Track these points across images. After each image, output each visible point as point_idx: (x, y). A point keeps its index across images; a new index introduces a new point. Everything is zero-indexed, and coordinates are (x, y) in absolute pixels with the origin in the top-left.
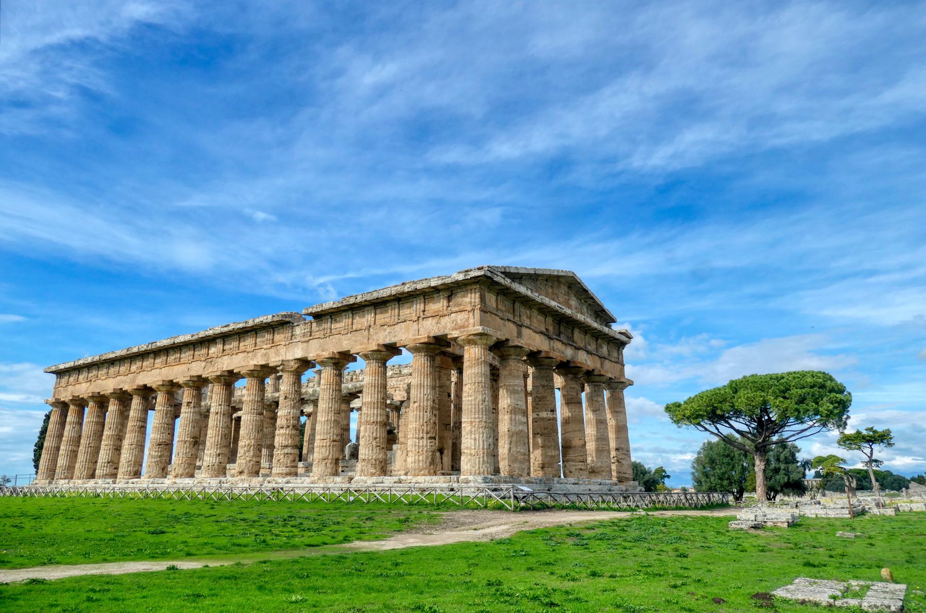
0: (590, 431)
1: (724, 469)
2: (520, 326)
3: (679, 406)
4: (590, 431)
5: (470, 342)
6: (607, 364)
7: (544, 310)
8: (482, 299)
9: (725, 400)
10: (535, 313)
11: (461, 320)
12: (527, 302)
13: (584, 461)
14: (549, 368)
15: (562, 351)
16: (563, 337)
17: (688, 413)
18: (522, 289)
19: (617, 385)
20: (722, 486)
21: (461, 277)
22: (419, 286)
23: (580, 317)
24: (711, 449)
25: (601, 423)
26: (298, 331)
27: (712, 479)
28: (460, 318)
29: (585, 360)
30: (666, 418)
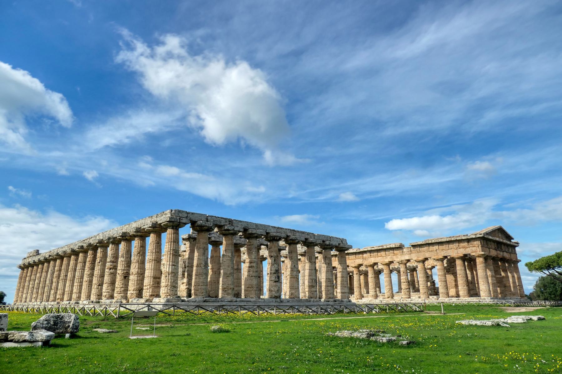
0: (511, 280)
1: (551, 290)
3: (532, 264)
5: (479, 256)
6: (512, 255)
9: (554, 262)
11: (475, 250)
13: (511, 291)
14: (498, 261)
15: (501, 254)
17: (537, 267)
18: (490, 237)
20: (551, 298)
21: (474, 237)
22: (458, 239)
24: (544, 280)
25: (513, 277)
26: (405, 250)
27: (545, 294)
28: (474, 249)
29: (506, 255)
30: (526, 268)
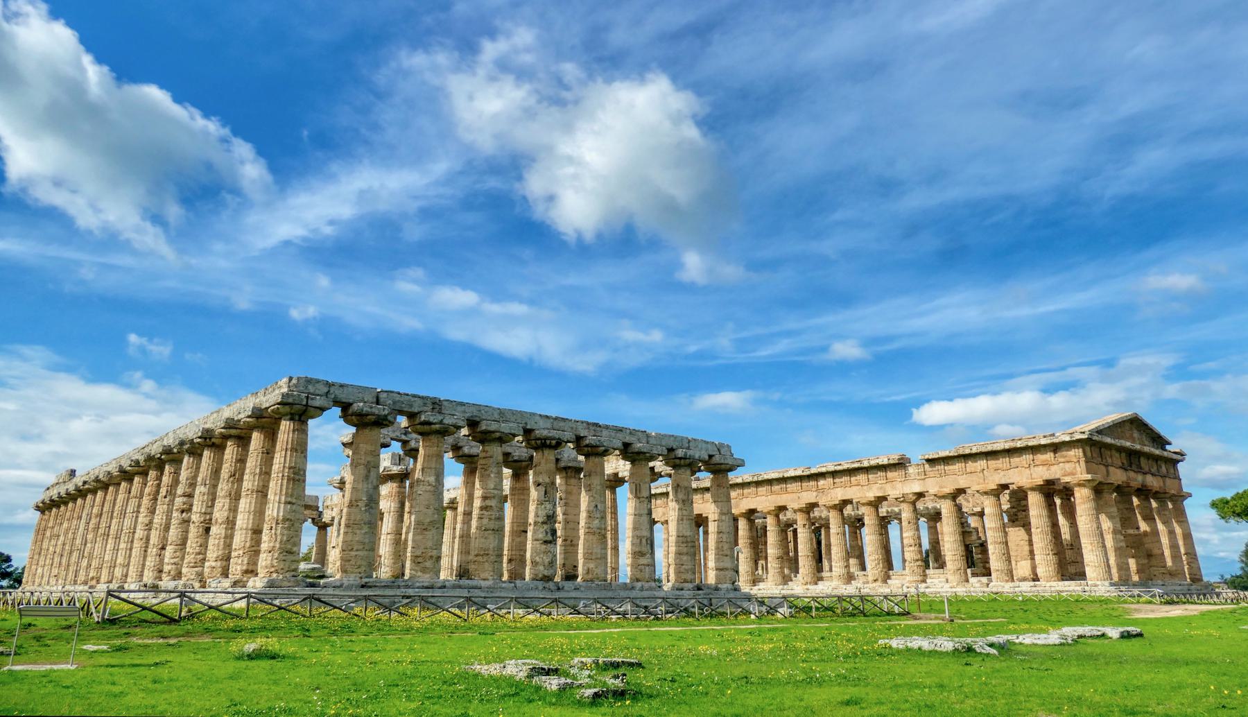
0: (1165, 540)
2: (1107, 466)
3: (1227, 502)
4: (1165, 540)
5: (1079, 485)
6: (1168, 481)
7: (1121, 450)
8: (1084, 452)
10: (1114, 452)
11: (1071, 469)
12: (1109, 447)
13: (1165, 566)
15: (1138, 479)
16: (1134, 467)
17: (1238, 510)
18: (1108, 440)
19: (1179, 498)
21: (1067, 439)
22: (1030, 444)
23: (1146, 449)
25: (1172, 533)
28: (1068, 467)
29: (1153, 482)
30: (1213, 514)
